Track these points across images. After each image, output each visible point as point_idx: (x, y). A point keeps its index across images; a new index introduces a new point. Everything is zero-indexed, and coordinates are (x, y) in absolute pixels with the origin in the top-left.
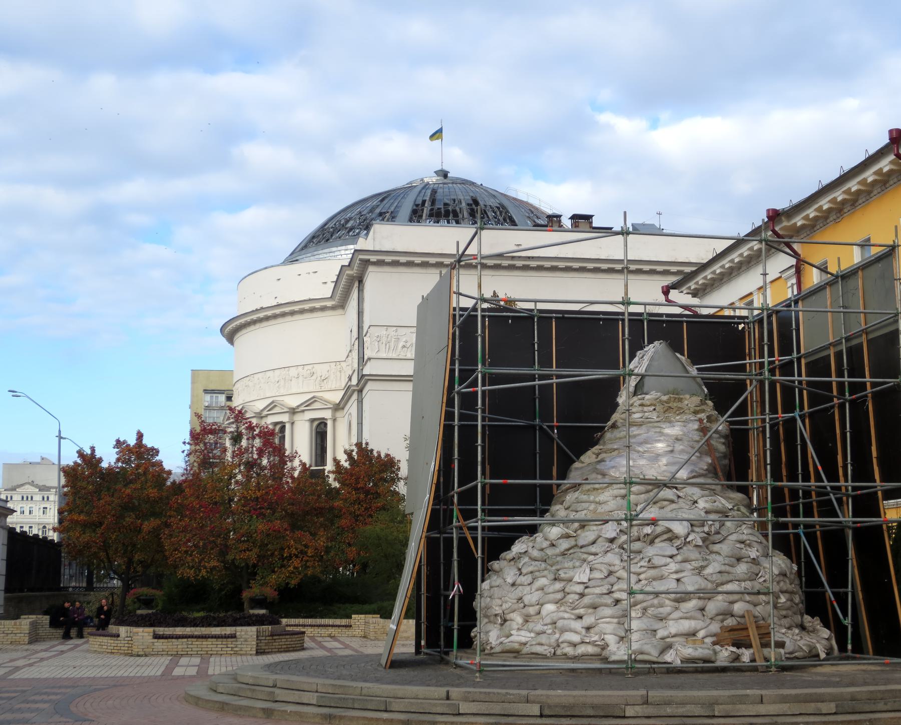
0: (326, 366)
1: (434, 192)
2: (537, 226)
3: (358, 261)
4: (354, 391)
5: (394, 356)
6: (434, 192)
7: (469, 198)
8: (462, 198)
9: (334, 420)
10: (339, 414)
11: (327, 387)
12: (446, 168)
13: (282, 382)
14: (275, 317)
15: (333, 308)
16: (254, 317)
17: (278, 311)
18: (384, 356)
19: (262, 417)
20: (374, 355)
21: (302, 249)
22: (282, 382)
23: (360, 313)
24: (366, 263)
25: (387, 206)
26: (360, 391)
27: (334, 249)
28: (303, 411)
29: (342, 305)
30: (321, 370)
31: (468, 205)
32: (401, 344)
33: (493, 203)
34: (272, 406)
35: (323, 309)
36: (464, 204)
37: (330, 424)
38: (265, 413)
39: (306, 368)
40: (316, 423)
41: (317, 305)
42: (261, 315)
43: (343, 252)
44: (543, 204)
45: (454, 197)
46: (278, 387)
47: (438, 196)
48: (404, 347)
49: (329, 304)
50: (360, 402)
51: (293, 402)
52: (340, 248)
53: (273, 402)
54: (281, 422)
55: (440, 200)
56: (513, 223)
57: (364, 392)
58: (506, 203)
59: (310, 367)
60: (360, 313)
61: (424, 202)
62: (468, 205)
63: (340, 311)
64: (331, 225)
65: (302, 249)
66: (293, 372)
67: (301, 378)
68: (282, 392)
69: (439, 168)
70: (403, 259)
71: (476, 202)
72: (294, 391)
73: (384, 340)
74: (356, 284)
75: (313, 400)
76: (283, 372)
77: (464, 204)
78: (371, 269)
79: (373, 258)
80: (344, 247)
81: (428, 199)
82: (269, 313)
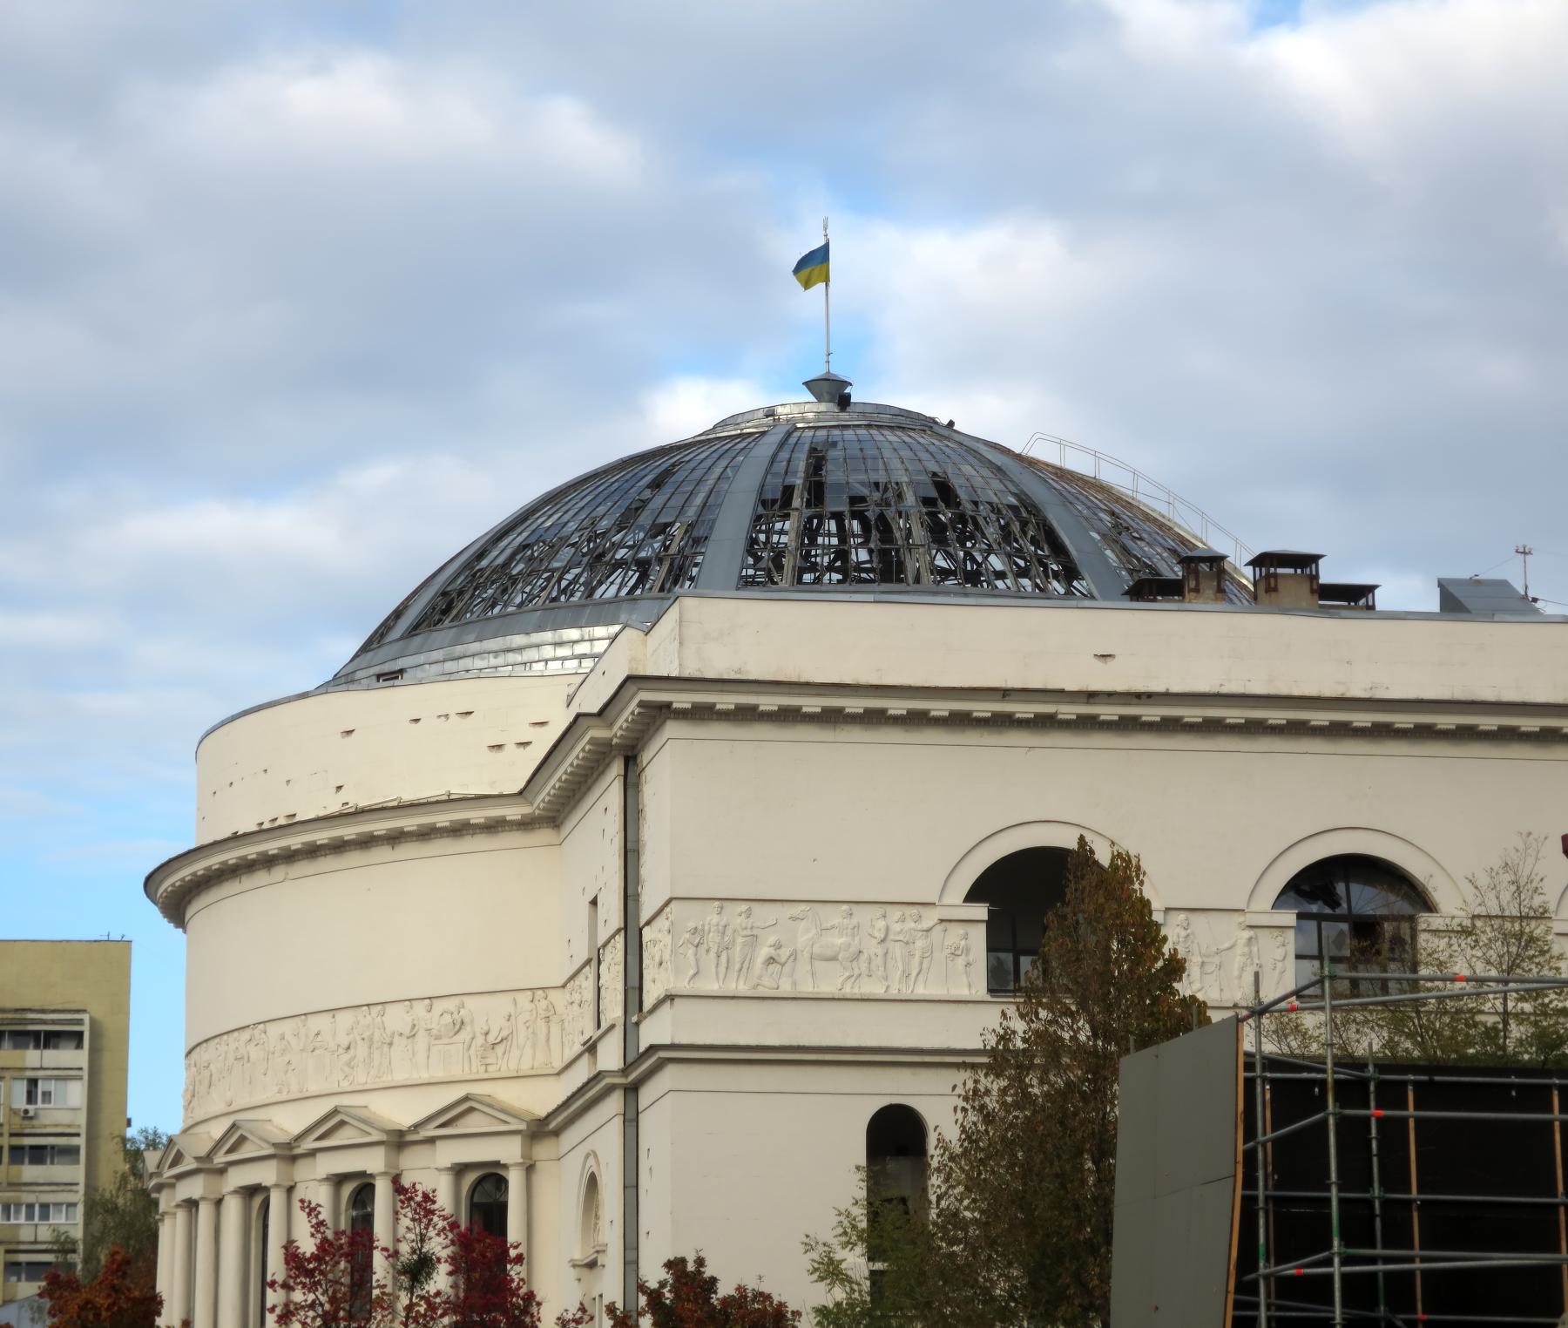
0: (503, 1004)
1: (817, 461)
2: (1149, 588)
3: (633, 706)
4: (610, 1089)
5: (743, 988)
6: (817, 461)
7: (925, 478)
8: (905, 479)
9: (530, 1169)
10: (543, 1150)
11: (509, 1065)
12: (840, 372)
13: (361, 1051)
14: (339, 847)
15: (526, 824)
16: (272, 846)
17: (349, 831)
18: (713, 987)
19: (294, 1159)
20: (682, 985)
21: (414, 630)
22: (361, 1051)
23: (631, 854)
24: (657, 714)
25: (678, 501)
26: (632, 1090)
27: (519, 640)
28: (432, 1141)
29: (555, 816)
30: (489, 1015)
31: (927, 501)
32: (764, 952)
33: (993, 491)
34: (333, 1122)
35: (494, 827)
36: (910, 499)
37: (515, 1179)
38: (309, 1144)
39: (439, 1006)
40: (470, 1178)
41: (477, 815)
42: (295, 842)
43: (548, 652)
44: (1143, 486)
45: (881, 478)
46: (349, 1064)
47: (833, 474)
48: (771, 960)
49: (513, 812)
50: (631, 1120)
51: (402, 1112)
52: (536, 637)
53: (335, 1112)
54: (362, 1174)
55: (839, 487)
56: (1070, 573)
57: (647, 1094)
58: (1038, 492)
59: (450, 1004)
60: (631, 854)
61: (788, 491)
62: (927, 501)
63: (545, 835)
64: (497, 556)
65: (414, 630)
66: (397, 1019)
67: (422, 1038)
68: (361, 1078)
69: (817, 372)
70: (768, 703)
71: (945, 490)
72: (399, 1077)
73: (713, 940)
74: (617, 768)
75: (465, 1107)
76: (366, 1018)
77: (910, 499)
78: (672, 729)
79: (682, 700)
80: (548, 636)
81: (799, 481)
82: (321, 836)
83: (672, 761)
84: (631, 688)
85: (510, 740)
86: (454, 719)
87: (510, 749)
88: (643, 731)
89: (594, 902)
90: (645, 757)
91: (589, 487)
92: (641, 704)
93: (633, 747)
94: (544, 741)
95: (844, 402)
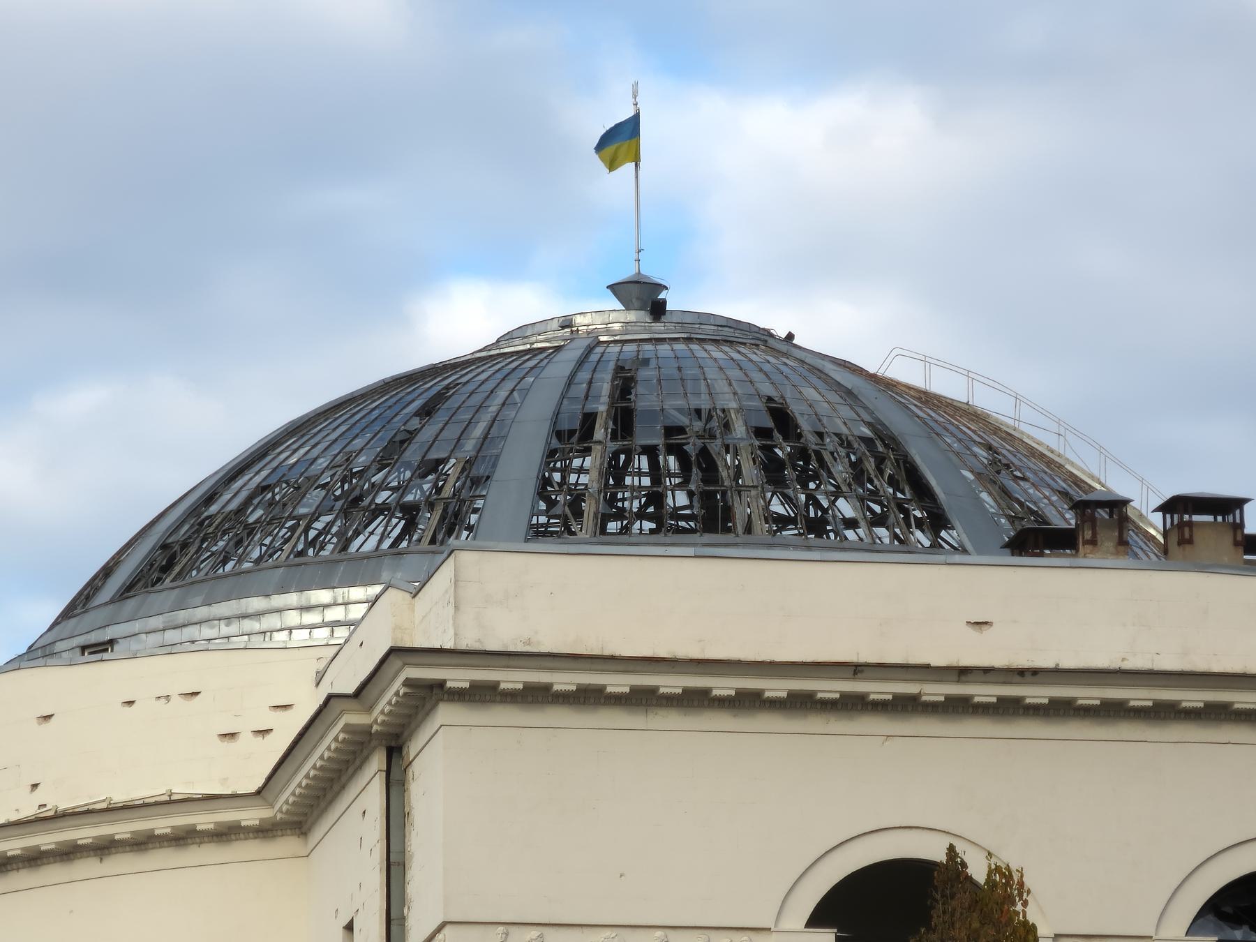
1: (625, 384)
2: (1034, 540)
3: (397, 685)
6: (625, 384)
7: (757, 404)
8: (733, 405)
12: (653, 273)
15: (265, 831)
17: (47, 840)
21: (128, 590)
23: (395, 868)
24: (429, 695)
25: (452, 432)
27: (256, 603)
29: (302, 821)
31: (761, 433)
33: (842, 420)
35: (225, 834)
36: (739, 429)
41: (205, 820)
43: (293, 618)
44: (1027, 413)
45: (704, 403)
47: (644, 399)
49: (250, 816)
52: (278, 600)
55: (652, 415)
56: (937, 521)
58: (897, 422)
60: (395, 868)
61: (589, 420)
62: (761, 433)
63: (289, 844)
64: (229, 500)
65: (128, 590)
70: (564, 681)
71: (782, 419)
74: (377, 762)
77: (739, 429)
78: (445, 713)
79: (458, 678)
80: (293, 598)
81: (602, 407)
83: (448, 754)
84: (395, 662)
85: (245, 727)
86: (176, 701)
87: (246, 738)
88: (410, 716)
89: (349, 927)
90: (412, 748)
91: (343, 415)
92: (408, 683)
93: (397, 736)
94: (288, 727)
95: (658, 310)
